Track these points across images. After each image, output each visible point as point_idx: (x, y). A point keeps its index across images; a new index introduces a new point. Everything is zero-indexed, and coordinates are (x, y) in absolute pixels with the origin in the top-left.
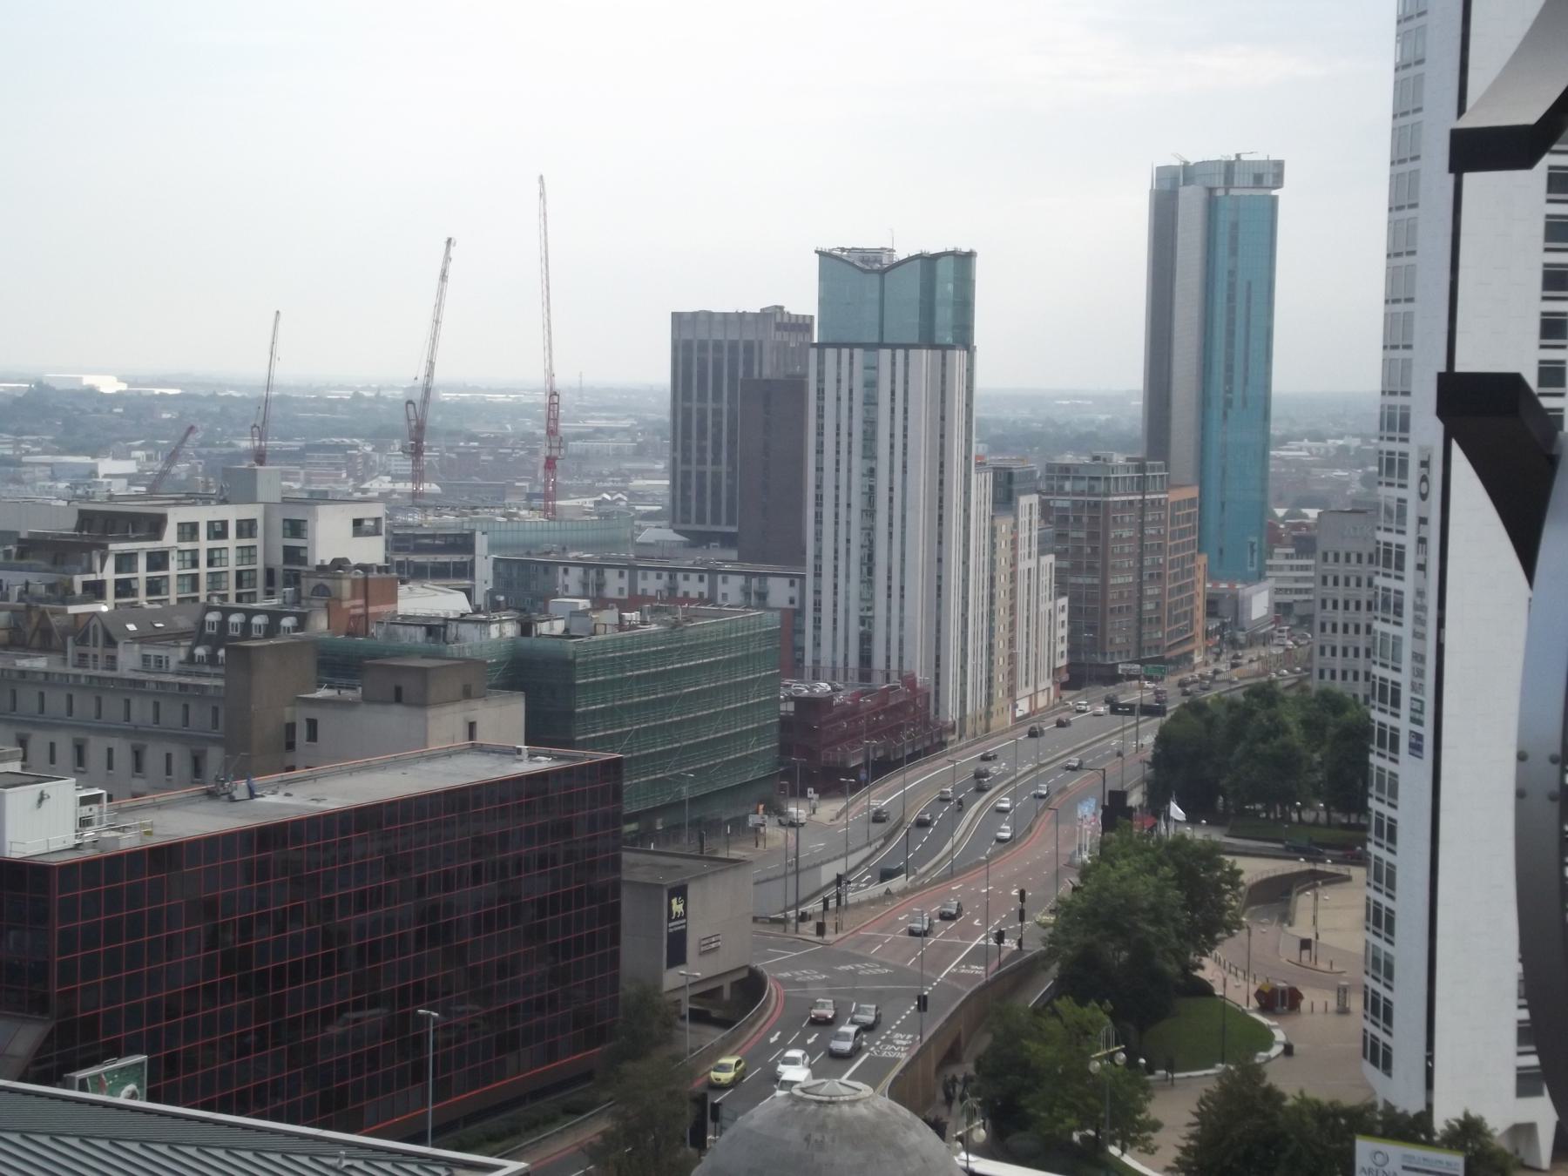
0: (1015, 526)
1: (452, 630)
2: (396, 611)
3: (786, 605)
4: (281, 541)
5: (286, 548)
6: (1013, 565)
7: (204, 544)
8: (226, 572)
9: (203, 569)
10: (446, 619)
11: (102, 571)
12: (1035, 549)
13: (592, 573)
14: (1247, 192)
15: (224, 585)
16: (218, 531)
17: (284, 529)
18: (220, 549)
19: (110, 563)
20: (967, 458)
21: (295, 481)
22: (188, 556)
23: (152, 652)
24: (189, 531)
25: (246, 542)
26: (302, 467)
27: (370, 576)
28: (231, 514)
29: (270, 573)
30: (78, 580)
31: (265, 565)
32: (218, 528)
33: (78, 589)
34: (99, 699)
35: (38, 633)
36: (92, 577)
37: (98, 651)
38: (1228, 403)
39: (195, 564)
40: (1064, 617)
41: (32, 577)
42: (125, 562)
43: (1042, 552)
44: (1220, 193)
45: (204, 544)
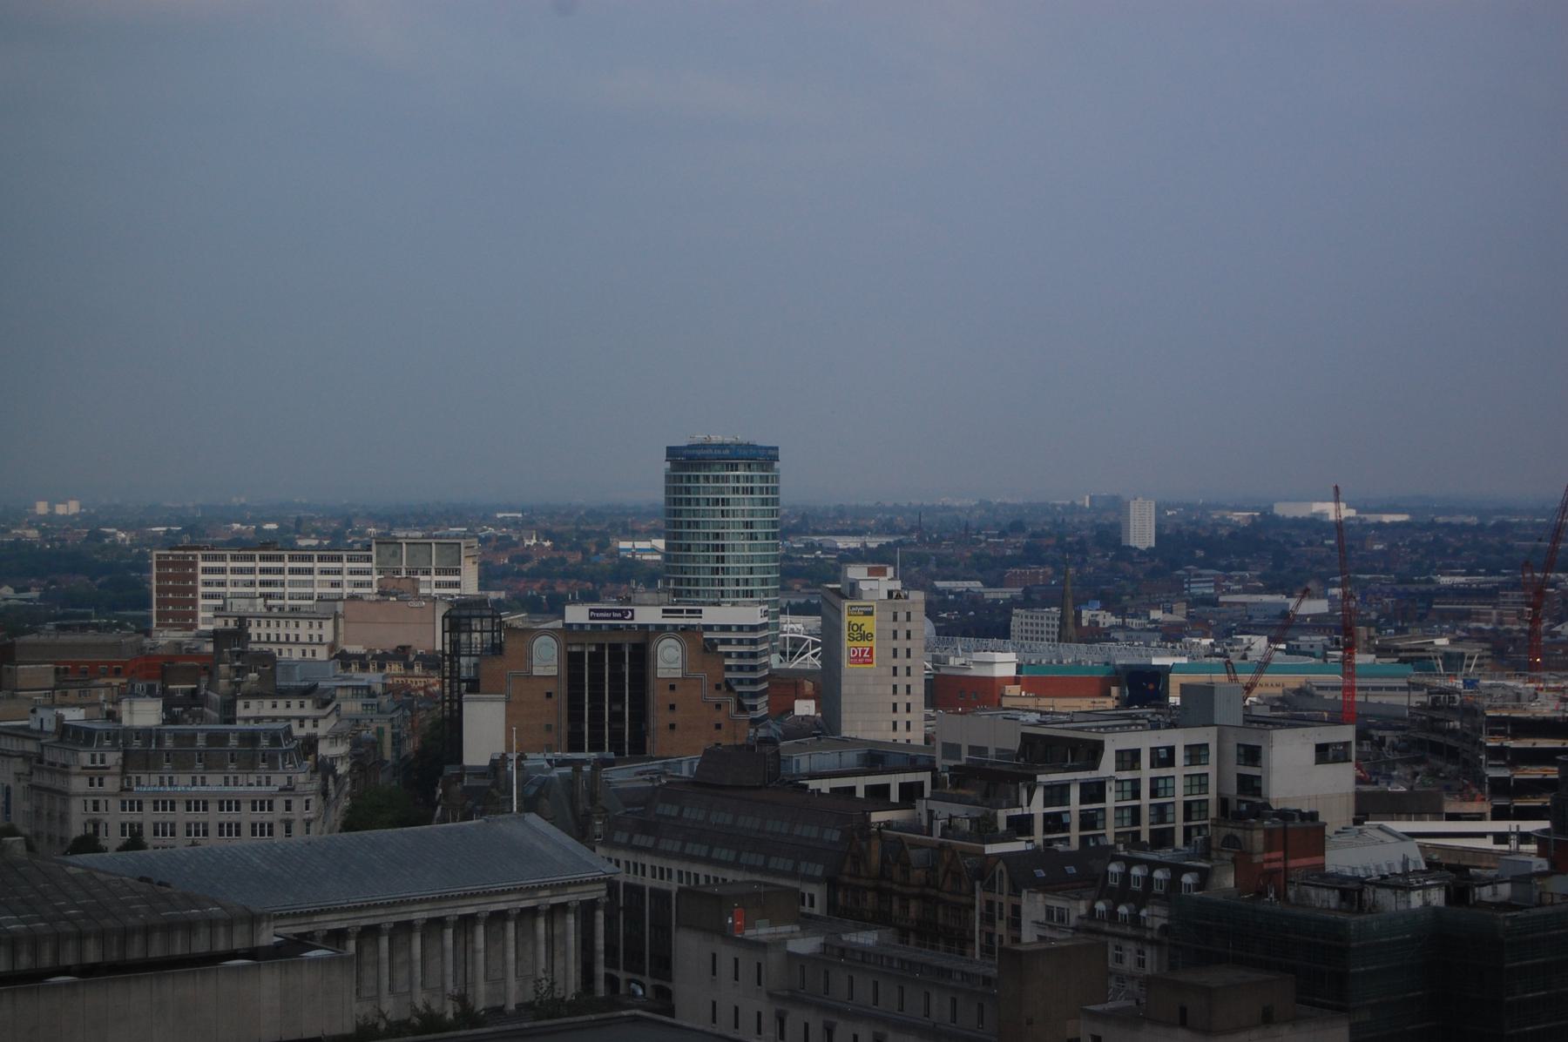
1: (1368, 895)
2: (1323, 866)
4: (1235, 769)
5: (1239, 775)
7: (1146, 772)
8: (1173, 803)
9: (1145, 799)
10: (1362, 882)
11: (1029, 805)
15: (1169, 818)
16: (1164, 758)
17: (1239, 755)
18: (1165, 778)
19: (1039, 795)
21: (1487, 622)
22: (1128, 786)
23: (1056, 903)
24: (1129, 759)
25: (1196, 770)
26: (1495, 606)
27: (1290, 825)
28: (1178, 739)
29: (1223, 802)
30: (1002, 815)
31: (1218, 794)
32: (1163, 754)
33: (1002, 825)
34: (901, 989)
35: (949, 875)
36: (1018, 812)
37: (1004, 899)
39: (1136, 794)
41: (958, 810)
42: (1057, 794)
45: (1146, 772)
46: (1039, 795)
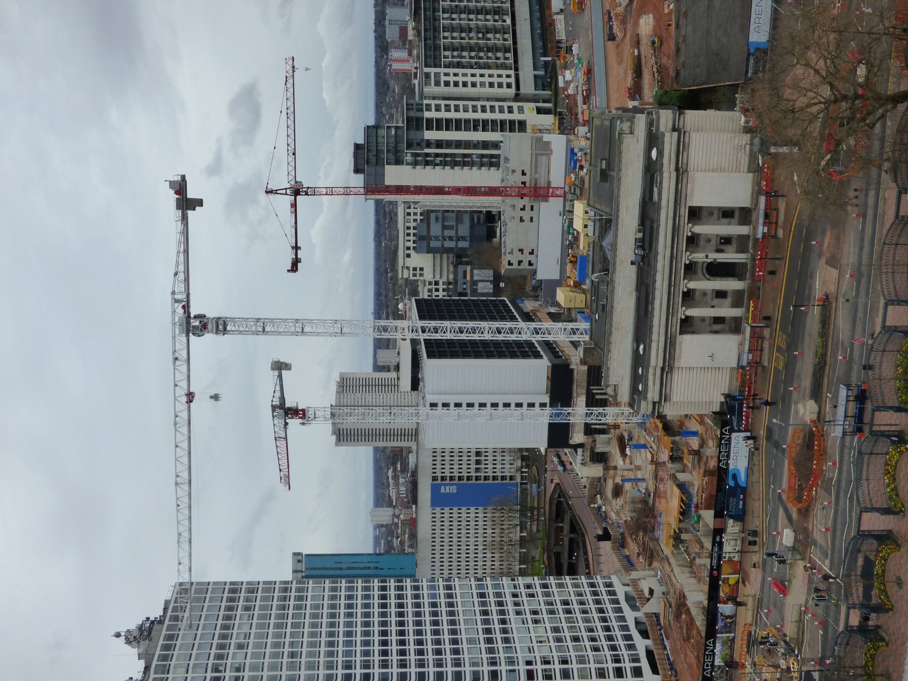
14: (304, 565)
38: (377, 568)
44: (304, 574)
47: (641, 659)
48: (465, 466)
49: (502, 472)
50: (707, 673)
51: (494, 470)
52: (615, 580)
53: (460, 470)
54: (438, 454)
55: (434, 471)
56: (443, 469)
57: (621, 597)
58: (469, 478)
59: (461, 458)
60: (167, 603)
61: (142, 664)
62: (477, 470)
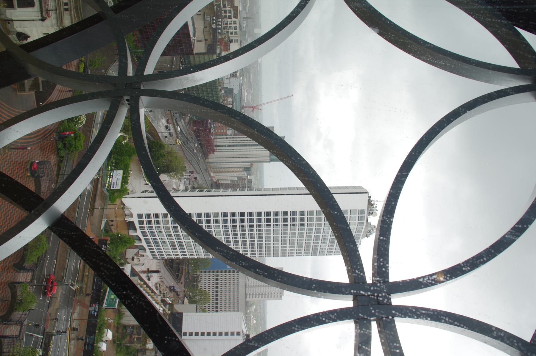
0: (242, 172)
3: (227, 133)
6: (236, 172)
7: (233, 25)
9: (229, 25)
12: (238, 176)
13: (231, 103)
16: (235, 28)
19: (229, 9)
20: (252, 162)
22: (231, 23)
36: (227, 6)
39: (230, 24)
40: (227, 182)
43: (238, 177)
45: (233, 25)
46: (229, 9)
47: (139, 228)
48: (223, 277)
49: (206, 275)
50: (104, 247)
51: (209, 276)
52: (151, 257)
53: (226, 275)
54: (236, 309)
55: (238, 275)
56: (234, 296)
57: (148, 251)
58: (222, 272)
59: (225, 281)
60: (360, 244)
61: (369, 221)
62: (217, 276)
